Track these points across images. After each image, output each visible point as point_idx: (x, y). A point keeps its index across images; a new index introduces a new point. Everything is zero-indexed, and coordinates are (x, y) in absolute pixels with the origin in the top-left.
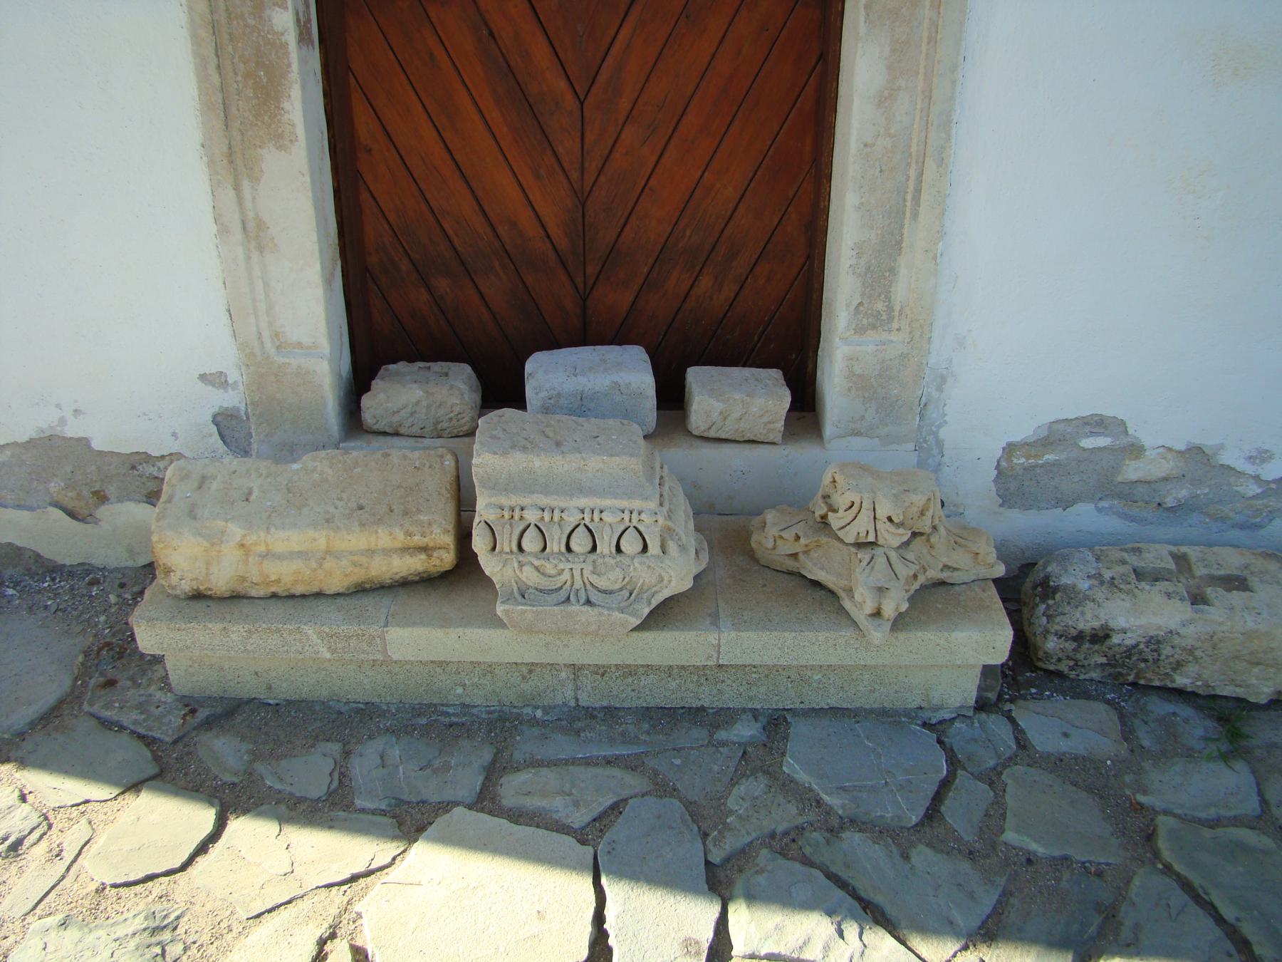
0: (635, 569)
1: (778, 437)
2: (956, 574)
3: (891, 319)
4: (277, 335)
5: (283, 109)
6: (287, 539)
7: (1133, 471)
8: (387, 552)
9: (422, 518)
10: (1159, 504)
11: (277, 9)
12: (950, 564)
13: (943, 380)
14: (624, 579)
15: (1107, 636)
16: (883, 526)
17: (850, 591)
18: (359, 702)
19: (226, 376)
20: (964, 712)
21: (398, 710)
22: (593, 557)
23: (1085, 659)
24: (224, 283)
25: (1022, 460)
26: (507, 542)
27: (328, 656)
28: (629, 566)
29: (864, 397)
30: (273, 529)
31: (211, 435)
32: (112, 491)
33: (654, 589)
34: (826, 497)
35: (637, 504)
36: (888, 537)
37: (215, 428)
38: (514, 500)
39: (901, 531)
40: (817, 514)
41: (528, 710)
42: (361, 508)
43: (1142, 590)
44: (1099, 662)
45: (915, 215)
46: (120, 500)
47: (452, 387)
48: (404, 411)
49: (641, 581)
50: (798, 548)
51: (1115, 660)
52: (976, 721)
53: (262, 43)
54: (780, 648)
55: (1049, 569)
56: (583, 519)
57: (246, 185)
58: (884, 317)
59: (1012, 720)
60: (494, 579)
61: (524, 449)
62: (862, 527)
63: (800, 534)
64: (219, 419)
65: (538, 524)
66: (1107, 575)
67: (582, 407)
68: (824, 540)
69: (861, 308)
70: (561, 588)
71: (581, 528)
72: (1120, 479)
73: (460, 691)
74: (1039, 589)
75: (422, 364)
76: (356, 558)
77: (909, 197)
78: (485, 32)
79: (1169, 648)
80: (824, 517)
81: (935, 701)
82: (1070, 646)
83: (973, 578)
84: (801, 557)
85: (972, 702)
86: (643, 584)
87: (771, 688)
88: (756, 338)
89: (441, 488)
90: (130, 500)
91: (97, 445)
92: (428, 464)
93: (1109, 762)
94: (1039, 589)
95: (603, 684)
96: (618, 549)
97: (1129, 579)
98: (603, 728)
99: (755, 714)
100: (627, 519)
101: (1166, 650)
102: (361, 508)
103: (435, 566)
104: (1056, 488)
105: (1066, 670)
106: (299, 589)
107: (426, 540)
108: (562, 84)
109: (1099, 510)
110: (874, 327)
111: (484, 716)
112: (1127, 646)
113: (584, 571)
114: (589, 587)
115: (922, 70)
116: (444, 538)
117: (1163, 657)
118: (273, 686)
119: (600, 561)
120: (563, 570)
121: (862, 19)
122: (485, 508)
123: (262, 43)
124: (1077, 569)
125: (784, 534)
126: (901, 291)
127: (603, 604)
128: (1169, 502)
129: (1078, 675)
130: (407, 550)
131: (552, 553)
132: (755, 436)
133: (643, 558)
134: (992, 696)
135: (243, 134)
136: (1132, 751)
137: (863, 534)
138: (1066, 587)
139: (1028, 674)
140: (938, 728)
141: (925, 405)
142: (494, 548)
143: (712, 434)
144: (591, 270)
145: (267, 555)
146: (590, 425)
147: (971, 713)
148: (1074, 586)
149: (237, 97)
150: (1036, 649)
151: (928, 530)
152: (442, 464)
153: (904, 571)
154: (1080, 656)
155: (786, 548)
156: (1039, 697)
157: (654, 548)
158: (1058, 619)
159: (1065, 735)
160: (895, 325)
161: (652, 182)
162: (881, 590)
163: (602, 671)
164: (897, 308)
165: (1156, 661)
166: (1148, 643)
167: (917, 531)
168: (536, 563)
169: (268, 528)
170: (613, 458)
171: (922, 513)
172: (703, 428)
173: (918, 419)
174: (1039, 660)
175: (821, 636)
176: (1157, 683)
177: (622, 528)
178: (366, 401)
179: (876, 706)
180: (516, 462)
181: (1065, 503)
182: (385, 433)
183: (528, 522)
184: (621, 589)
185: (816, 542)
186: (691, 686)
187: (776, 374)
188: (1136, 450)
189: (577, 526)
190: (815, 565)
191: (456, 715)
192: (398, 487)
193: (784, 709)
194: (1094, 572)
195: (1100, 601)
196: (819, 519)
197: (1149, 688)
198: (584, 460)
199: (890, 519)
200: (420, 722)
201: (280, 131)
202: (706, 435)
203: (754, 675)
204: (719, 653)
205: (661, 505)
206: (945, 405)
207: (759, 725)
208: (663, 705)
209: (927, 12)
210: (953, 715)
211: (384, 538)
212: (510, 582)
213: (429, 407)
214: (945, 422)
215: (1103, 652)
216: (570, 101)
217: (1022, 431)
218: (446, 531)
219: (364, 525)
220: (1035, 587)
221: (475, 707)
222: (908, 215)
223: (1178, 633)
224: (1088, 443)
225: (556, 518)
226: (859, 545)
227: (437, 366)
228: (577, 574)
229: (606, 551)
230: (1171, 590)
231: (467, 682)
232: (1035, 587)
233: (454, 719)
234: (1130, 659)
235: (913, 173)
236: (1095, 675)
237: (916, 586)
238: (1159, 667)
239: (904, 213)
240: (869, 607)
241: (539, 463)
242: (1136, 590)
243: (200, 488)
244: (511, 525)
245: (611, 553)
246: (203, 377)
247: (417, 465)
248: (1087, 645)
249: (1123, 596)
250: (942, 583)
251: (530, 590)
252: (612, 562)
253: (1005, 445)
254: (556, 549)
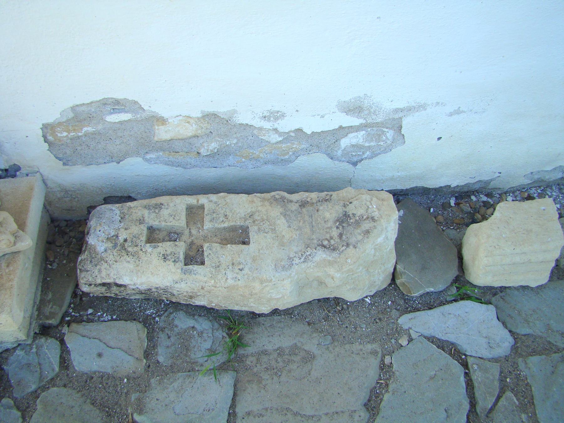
25: (65, 134)
43: (146, 252)
72: (156, 139)
195: (111, 262)
210: (15, 345)
242: (141, 252)
253: (41, 126)
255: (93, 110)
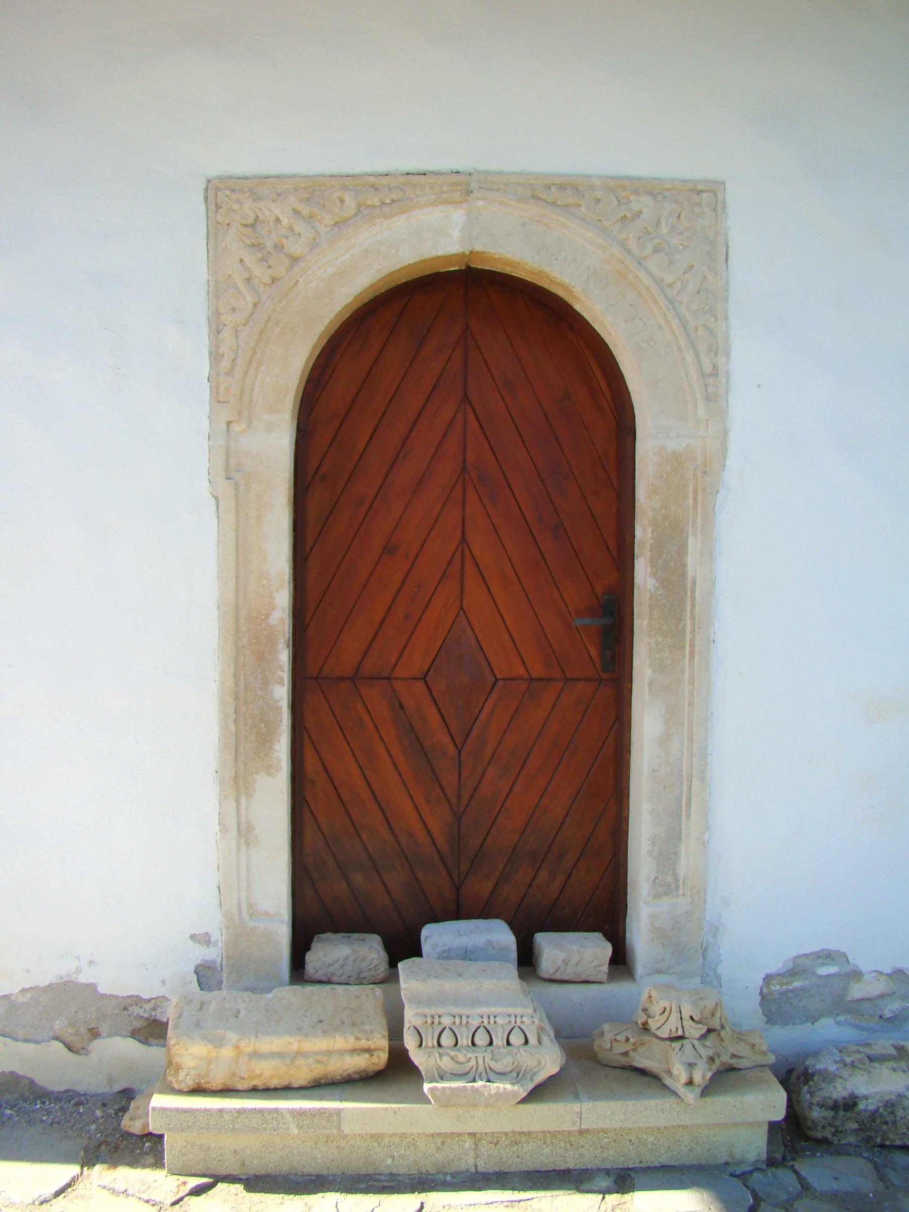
0: (521, 1056)
1: (604, 977)
2: (741, 1060)
3: (677, 887)
4: (250, 906)
5: (274, 749)
6: (267, 1044)
7: (857, 991)
8: (341, 1052)
9: (366, 1028)
10: (881, 1016)
11: (278, 685)
12: (736, 1053)
13: (717, 930)
14: (513, 1063)
15: (855, 1104)
16: (688, 1023)
17: (669, 1072)
18: (311, 1175)
19: (210, 937)
20: (759, 1165)
21: (342, 1179)
22: (491, 1048)
23: (842, 1125)
24: (218, 868)
25: (778, 987)
26: (430, 1041)
27: (296, 1131)
28: (517, 1054)
29: (663, 944)
30: (260, 1036)
31: (191, 982)
32: (104, 1029)
33: (535, 1070)
34: (645, 1010)
35: (519, 1010)
36: (692, 1031)
37: (196, 976)
38: (434, 1010)
39: (700, 1026)
40: (639, 1022)
41: (441, 1176)
42: (321, 1021)
43: (874, 1068)
44: (853, 1128)
45: (688, 816)
46: (110, 1035)
47: (371, 947)
48: (337, 964)
49: (525, 1064)
50: (627, 1047)
51: (865, 1125)
52: (768, 1172)
53: (265, 706)
54: (624, 1114)
55: (807, 1063)
56: (483, 1022)
57: (243, 799)
58: (673, 886)
59: (796, 1172)
60: (421, 1068)
61: (436, 977)
62: (672, 1026)
63: (629, 1036)
64: (199, 969)
65: (451, 1026)
66: (848, 1060)
67: (467, 955)
68: (646, 1038)
69: (657, 881)
70: (469, 1072)
71: (482, 1029)
72: (849, 998)
73: (389, 1162)
74: (802, 1078)
75: (344, 934)
76: (319, 1057)
77: (684, 804)
78: (397, 704)
79: (901, 1110)
80: (645, 1024)
81: (738, 1157)
82: (829, 1114)
83: (753, 1064)
84: (631, 1053)
85: (764, 1156)
86: (527, 1067)
87: (618, 1150)
88: (580, 915)
90: (117, 1035)
91: (102, 989)
92: (364, 994)
93: (871, 1195)
94: (802, 1078)
95: (496, 1151)
96: (508, 1043)
97: (864, 1062)
99: (608, 1172)
100: (513, 1020)
101: (900, 1113)
102: (321, 1021)
103: (374, 1064)
104: (805, 1007)
105: (829, 1136)
106: (274, 1083)
107: (370, 1043)
108: (447, 740)
109: (838, 1023)
110: (666, 894)
111: (407, 1181)
112: (870, 1111)
113: (486, 1059)
114: (488, 1070)
115: (686, 723)
116: (381, 1042)
117: (898, 1118)
118: (247, 1163)
119: (496, 1051)
120: (470, 1058)
121: (647, 692)
122: (410, 1016)
123: (265, 706)
124: (827, 1059)
125: (618, 1038)
126: (682, 868)
128: (887, 1014)
129: (839, 1141)
130: (354, 1051)
131: (462, 1046)
132: (589, 976)
133: (526, 1047)
134: (778, 1156)
135: (245, 765)
136: (887, 1188)
137: (674, 1030)
138: (820, 1072)
139: (803, 1143)
140: (743, 1177)
141: (706, 948)
142: (421, 1045)
143: (558, 976)
144: (464, 867)
145: (255, 1055)
146: (480, 965)
147: (764, 1167)
148: (826, 1070)
149: (245, 740)
150: (805, 1119)
151: (718, 1027)
152: (374, 994)
153: (705, 1053)
154: (838, 1123)
155: (619, 1048)
156: (814, 1155)
157: (533, 1040)
158: (818, 1093)
159: (836, 1179)
160: (681, 892)
161: (506, 804)
162: (691, 1065)
163: (495, 1139)
164: (681, 880)
165: (894, 1122)
166: (885, 1106)
167: (711, 1027)
168: (452, 1053)
169: (256, 1034)
170: (500, 981)
171: (713, 1015)
172: (551, 972)
173: (701, 959)
174: (809, 1128)
175: (653, 1102)
176: (898, 1143)
177: (510, 1028)
178: (309, 957)
179: (694, 1163)
180: (432, 986)
181: (813, 1018)
182: (320, 982)
183: (444, 1026)
184: (511, 1071)
185: (641, 1041)
186: (561, 1152)
187: (598, 936)
188: (856, 975)
189: (479, 1028)
191: (387, 1181)
192: (345, 1008)
193: (628, 1169)
194: (838, 1059)
196: (641, 1026)
197: (894, 1147)
199: (692, 1018)
200: (362, 1186)
201: (270, 763)
202: (553, 977)
203: (605, 1140)
204: (581, 1119)
205: (535, 1011)
206: (719, 948)
207: (611, 1178)
208: (539, 1169)
209: (686, 686)
210: (751, 1168)
211: (341, 1042)
212: (432, 1069)
213: (355, 961)
214: (721, 961)
215: (855, 1118)
216: (452, 750)
217: (775, 965)
218: (384, 1037)
219: (326, 1032)
220: (798, 1078)
221: (399, 1175)
222: (684, 815)
223: (905, 1096)
224: (822, 971)
225: (464, 1022)
226: (672, 1039)
227: (355, 936)
228: (480, 1060)
229: (500, 1044)
230: (895, 1066)
231: (395, 1154)
232: (798, 1078)
233: (387, 1184)
234: (875, 1122)
235: (685, 788)
236: (851, 1139)
237: (714, 1068)
238: (897, 1128)
239: (681, 815)
240: (684, 1079)
241: (449, 986)
243: (201, 1009)
244: (433, 1028)
245: (503, 1045)
246: (193, 937)
247: (357, 994)
248: (841, 1113)
249: (861, 1072)
250: (732, 1069)
251: (447, 1075)
252: (504, 1051)
253: (764, 976)
254: (465, 1043)
255: (808, 963)
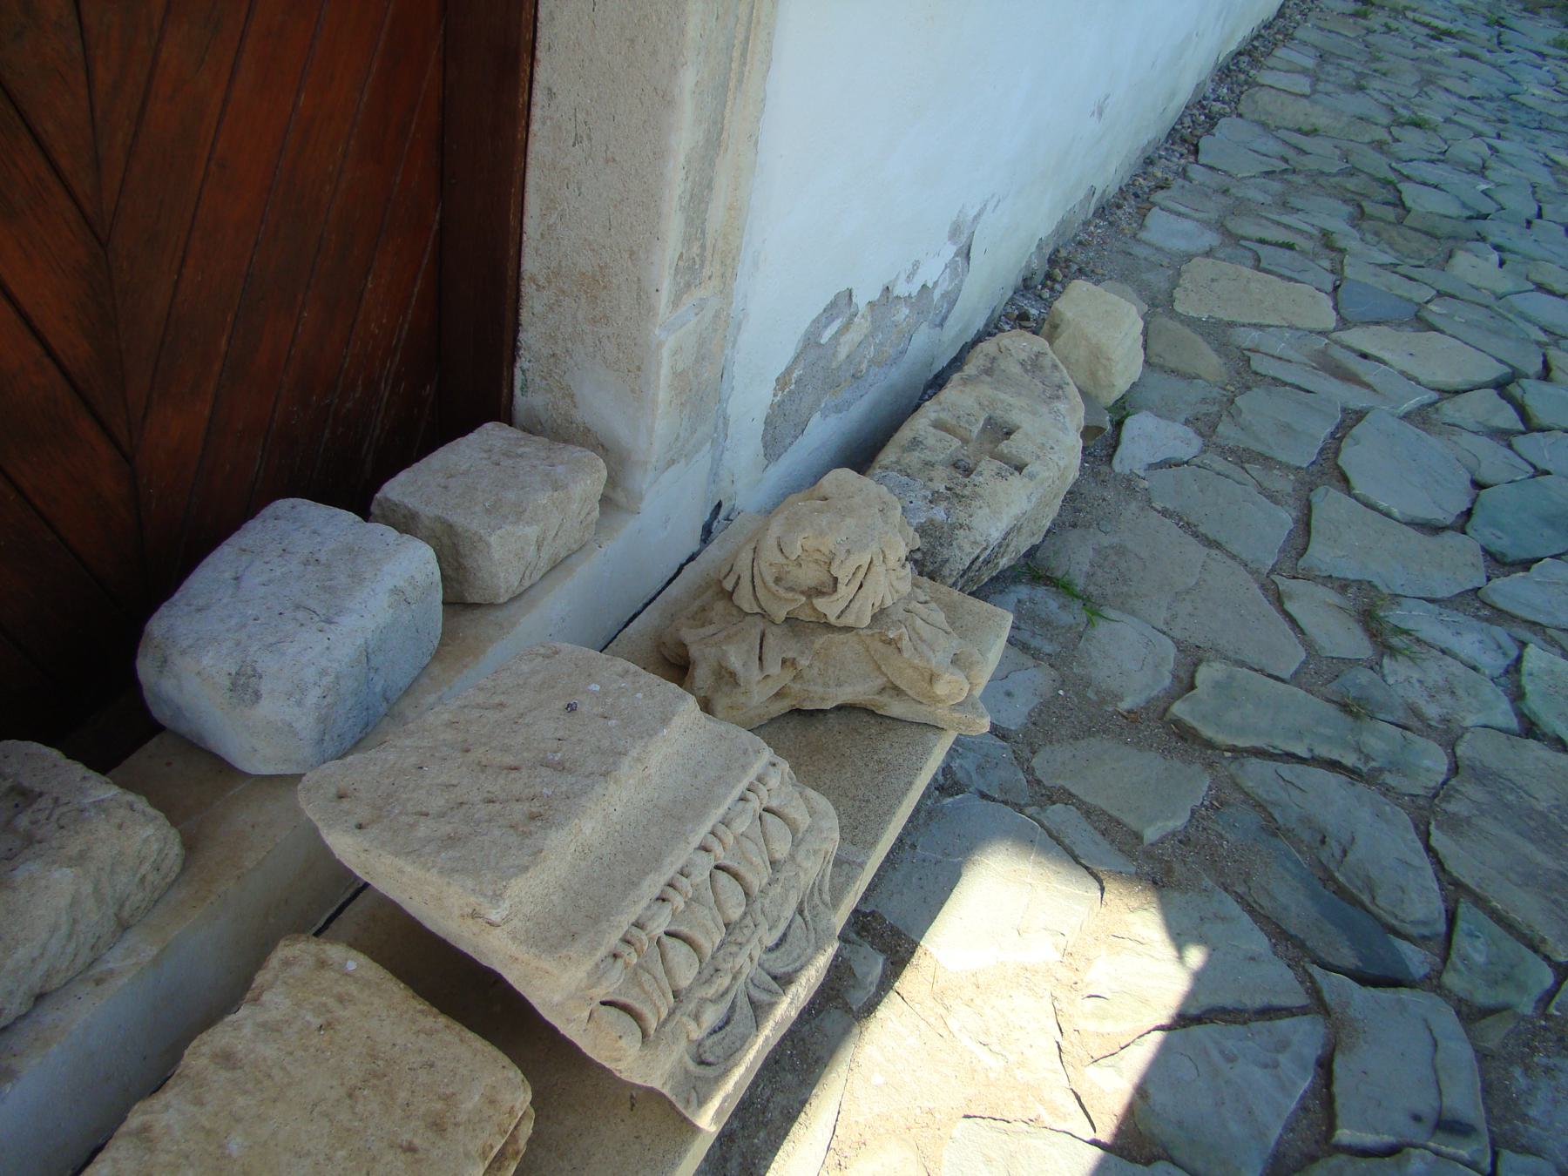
9: (469, 1105)
65: (673, 928)
89: (414, 1021)
92: (332, 1003)
98: (762, 1134)
127: (797, 964)
158: (946, 572)
168: (711, 991)
190: (826, 685)
192: (350, 1096)
198: (639, 760)
213: (96, 890)
247: (317, 1022)
